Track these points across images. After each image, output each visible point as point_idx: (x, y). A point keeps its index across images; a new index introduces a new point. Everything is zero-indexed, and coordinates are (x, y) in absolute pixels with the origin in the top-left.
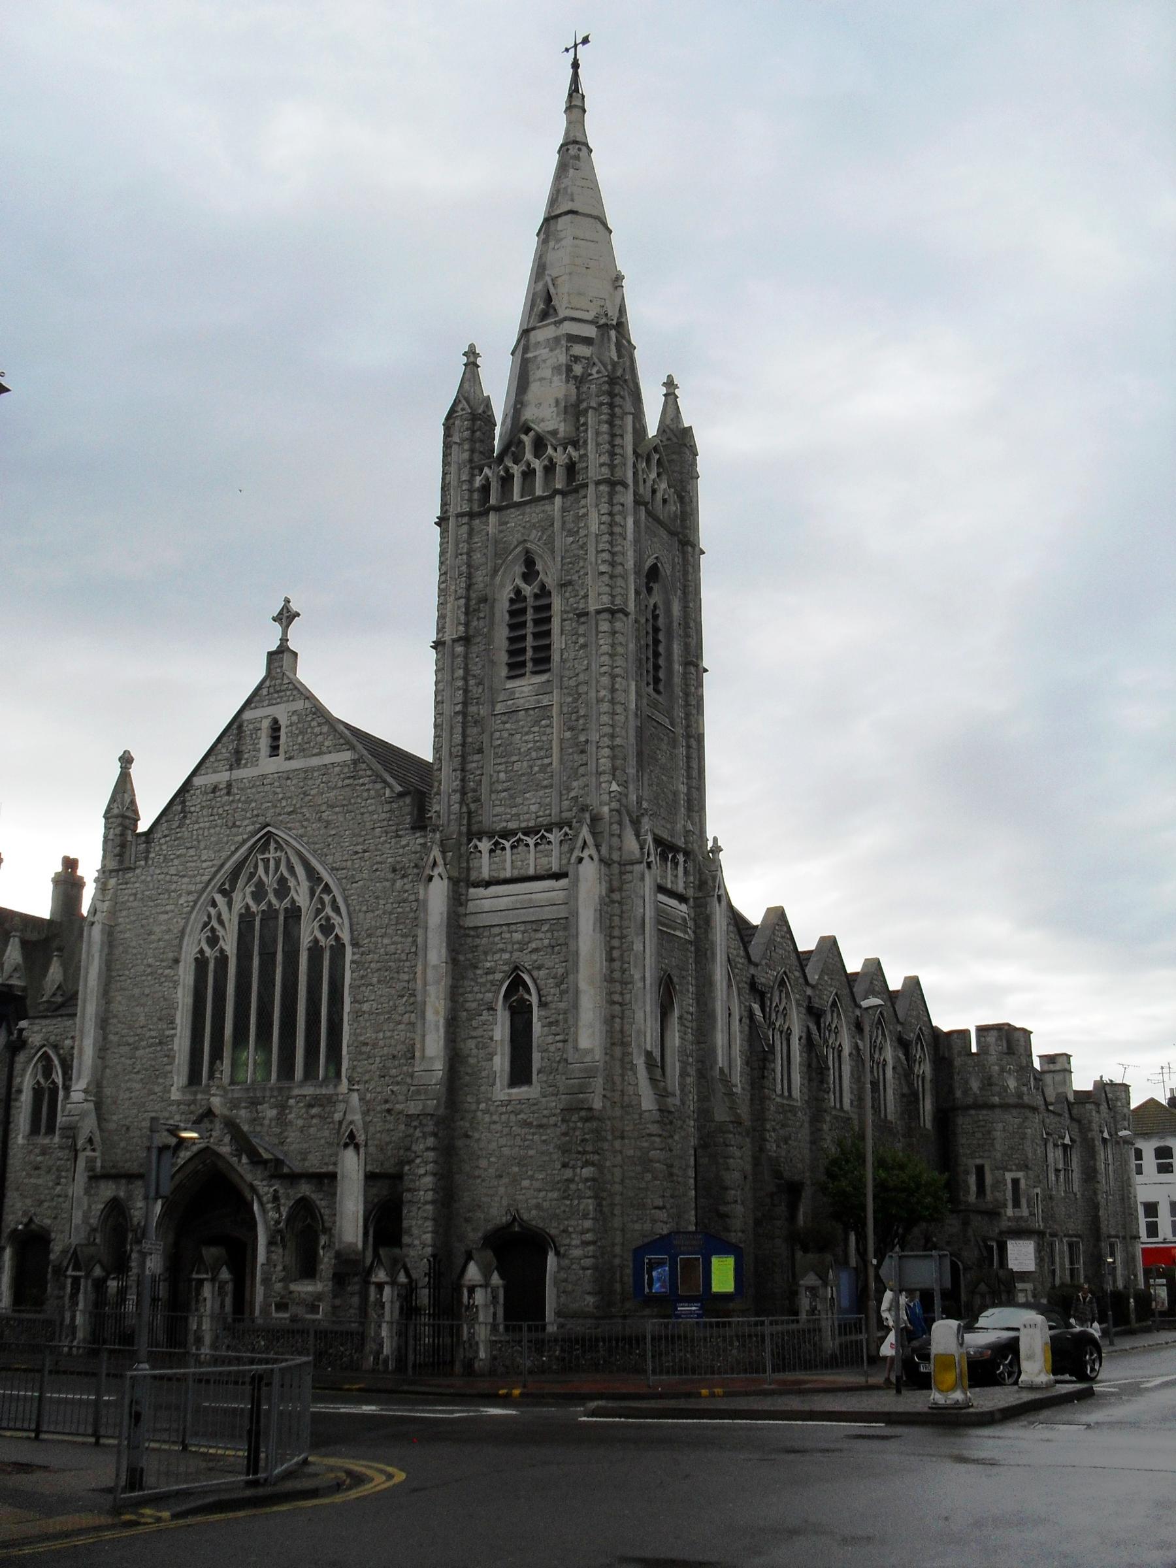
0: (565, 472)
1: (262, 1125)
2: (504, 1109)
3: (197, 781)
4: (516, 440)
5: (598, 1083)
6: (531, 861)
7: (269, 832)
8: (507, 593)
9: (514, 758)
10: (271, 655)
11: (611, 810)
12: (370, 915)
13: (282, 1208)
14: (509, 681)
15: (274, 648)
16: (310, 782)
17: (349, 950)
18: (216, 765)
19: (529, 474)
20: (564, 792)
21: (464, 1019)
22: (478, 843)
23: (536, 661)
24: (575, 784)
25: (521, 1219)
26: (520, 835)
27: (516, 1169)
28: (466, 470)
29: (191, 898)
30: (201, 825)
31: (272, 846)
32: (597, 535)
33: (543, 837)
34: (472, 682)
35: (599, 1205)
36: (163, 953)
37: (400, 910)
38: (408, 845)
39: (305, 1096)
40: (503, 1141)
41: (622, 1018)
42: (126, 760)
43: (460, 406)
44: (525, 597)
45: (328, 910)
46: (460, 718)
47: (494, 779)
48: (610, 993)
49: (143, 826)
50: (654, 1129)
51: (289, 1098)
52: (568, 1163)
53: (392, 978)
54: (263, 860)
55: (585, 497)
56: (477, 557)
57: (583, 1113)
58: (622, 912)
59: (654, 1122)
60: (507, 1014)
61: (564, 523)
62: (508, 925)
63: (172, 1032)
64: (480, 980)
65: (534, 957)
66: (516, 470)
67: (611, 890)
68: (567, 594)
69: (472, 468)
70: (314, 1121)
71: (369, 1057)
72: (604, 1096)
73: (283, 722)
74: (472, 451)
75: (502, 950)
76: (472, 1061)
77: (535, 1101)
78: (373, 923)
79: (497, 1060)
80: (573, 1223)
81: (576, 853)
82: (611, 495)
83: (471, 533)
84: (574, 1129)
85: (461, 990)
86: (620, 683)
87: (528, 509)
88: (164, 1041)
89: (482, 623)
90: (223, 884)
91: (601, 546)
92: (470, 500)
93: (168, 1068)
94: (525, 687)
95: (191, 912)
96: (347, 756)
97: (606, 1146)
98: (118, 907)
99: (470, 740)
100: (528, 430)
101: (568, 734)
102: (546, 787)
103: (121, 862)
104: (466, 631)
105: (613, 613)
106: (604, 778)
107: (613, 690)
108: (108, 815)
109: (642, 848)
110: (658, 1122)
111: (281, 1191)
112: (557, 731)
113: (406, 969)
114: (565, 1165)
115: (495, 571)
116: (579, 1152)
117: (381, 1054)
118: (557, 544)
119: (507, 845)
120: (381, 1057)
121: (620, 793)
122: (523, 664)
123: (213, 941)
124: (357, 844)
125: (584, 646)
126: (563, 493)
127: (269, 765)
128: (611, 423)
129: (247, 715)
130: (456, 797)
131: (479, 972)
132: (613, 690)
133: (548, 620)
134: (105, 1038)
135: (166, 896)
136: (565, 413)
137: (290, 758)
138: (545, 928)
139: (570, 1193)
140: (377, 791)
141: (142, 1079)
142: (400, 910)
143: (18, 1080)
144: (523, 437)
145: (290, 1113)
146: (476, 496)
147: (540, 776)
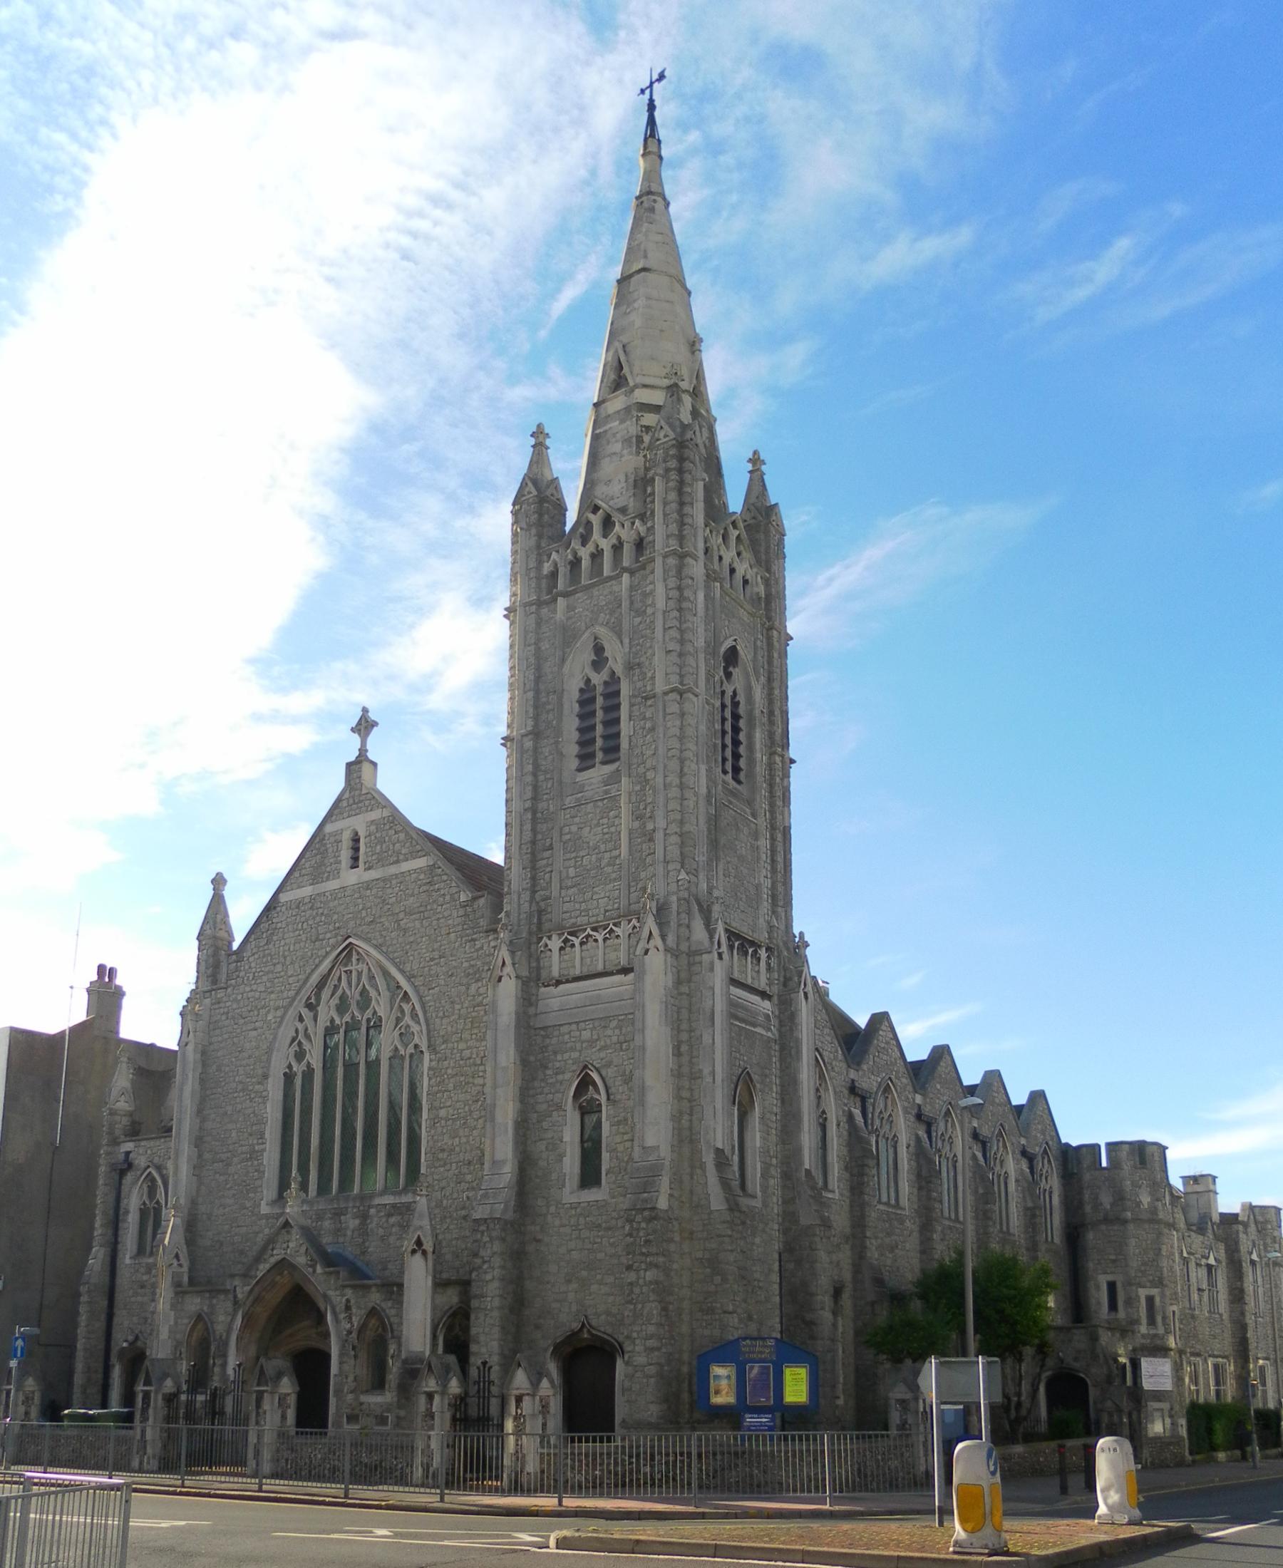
0: (634, 547)
2: (573, 1212)
3: (283, 898)
4: (584, 521)
5: (664, 1183)
6: (599, 955)
7: (350, 943)
9: (581, 854)
10: (349, 765)
11: (679, 900)
12: (445, 1021)
13: (354, 1318)
14: (579, 774)
15: (352, 759)
16: (389, 891)
17: (427, 1057)
18: (301, 879)
19: (597, 556)
20: (632, 884)
21: (534, 1121)
22: (548, 942)
23: (606, 751)
24: (643, 875)
25: (590, 1326)
27: (584, 1273)
28: (533, 557)
29: (279, 1013)
30: (287, 941)
31: (355, 957)
32: (664, 612)
33: (612, 931)
34: (541, 778)
35: (665, 1309)
36: (253, 1069)
37: (474, 1014)
38: (482, 948)
39: (386, 1205)
40: (572, 1245)
41: (691, 1115)
42: (219, 882)
43: (527, 489)
44: (595, 685)
45: (407, 1019)
46: (529, 816)
47: (564, 875)
48: (679, 1089)
49: (235, 946)
51: (370, 1207)
52: (632, 1266)
53: (468, 1083)
54: (346, 972)
55: (653, 572)
56: (545, 646)
57: (646, 1213)
58: (690, 1004)
59: (724, 1222)
61: (632, 603)
63: (263, 1146)
64: (550, 1081)
65: (602, 1055)
66: (585, 553)
67: (678, 982)
68: (636, 678)
69: (539, 554)
70: (394, 1230)
71: (445, 1164)
72: (671, 1195)
73: (362, 834)
74: (540, 536)
76: (542, 1163)
77: (603, 1203)
78: (449, 1028)
79: (567, 1160)
80: (637, 1328)
81: (642, 945)
82: (680, 569)
83: (539, 624)
84: (638, 1230)
85: (531, 1092)
86: (691, 766)
87: (595, 592)
88: (254, 1155)
89: (551, 716)
90: (309, 998)
91: (669, 624)
92: (539, 587)
93: (258, 1183)
96: (421, 863)
97: (672, 1247)
99: (539, 837)
100: (596, 509)
101: (636, 824)
102: (615, 880)
104: (536, 725)
107: (682, 774)
108: (200, 937)
109: (711, 937)
111: (353, 1302)
112: (625, 821)
113: (481, 1074)
114: (629, 1268)
115: (563, 660)
116: (643, 1254)
117: (457, 1160)
118: (626, 626)
119: (577, 941)
120: (457, 1163)
122: (592, 756)
123: (300, 1055)
124: (433, 950)
125: (653, 729)
126: (632, 572)
127: (351, 877)
128: (680, 492)
129: (329, 828)
130: (526, 896)
131: (549, 1072)
132: (682, 774)
133: (617, 707)
134: (200, 1156)
135: (256, 1013)
136: (635, 486)
137: (369, 868)
138: (614, 1024)
139: (634, 1297)
141: (234, 1195)
142: (474, 1014)
143: (125, 1201)
144: (591, 517)
145: (371, 1223)
146: (544, 583)
147: (609, 869)
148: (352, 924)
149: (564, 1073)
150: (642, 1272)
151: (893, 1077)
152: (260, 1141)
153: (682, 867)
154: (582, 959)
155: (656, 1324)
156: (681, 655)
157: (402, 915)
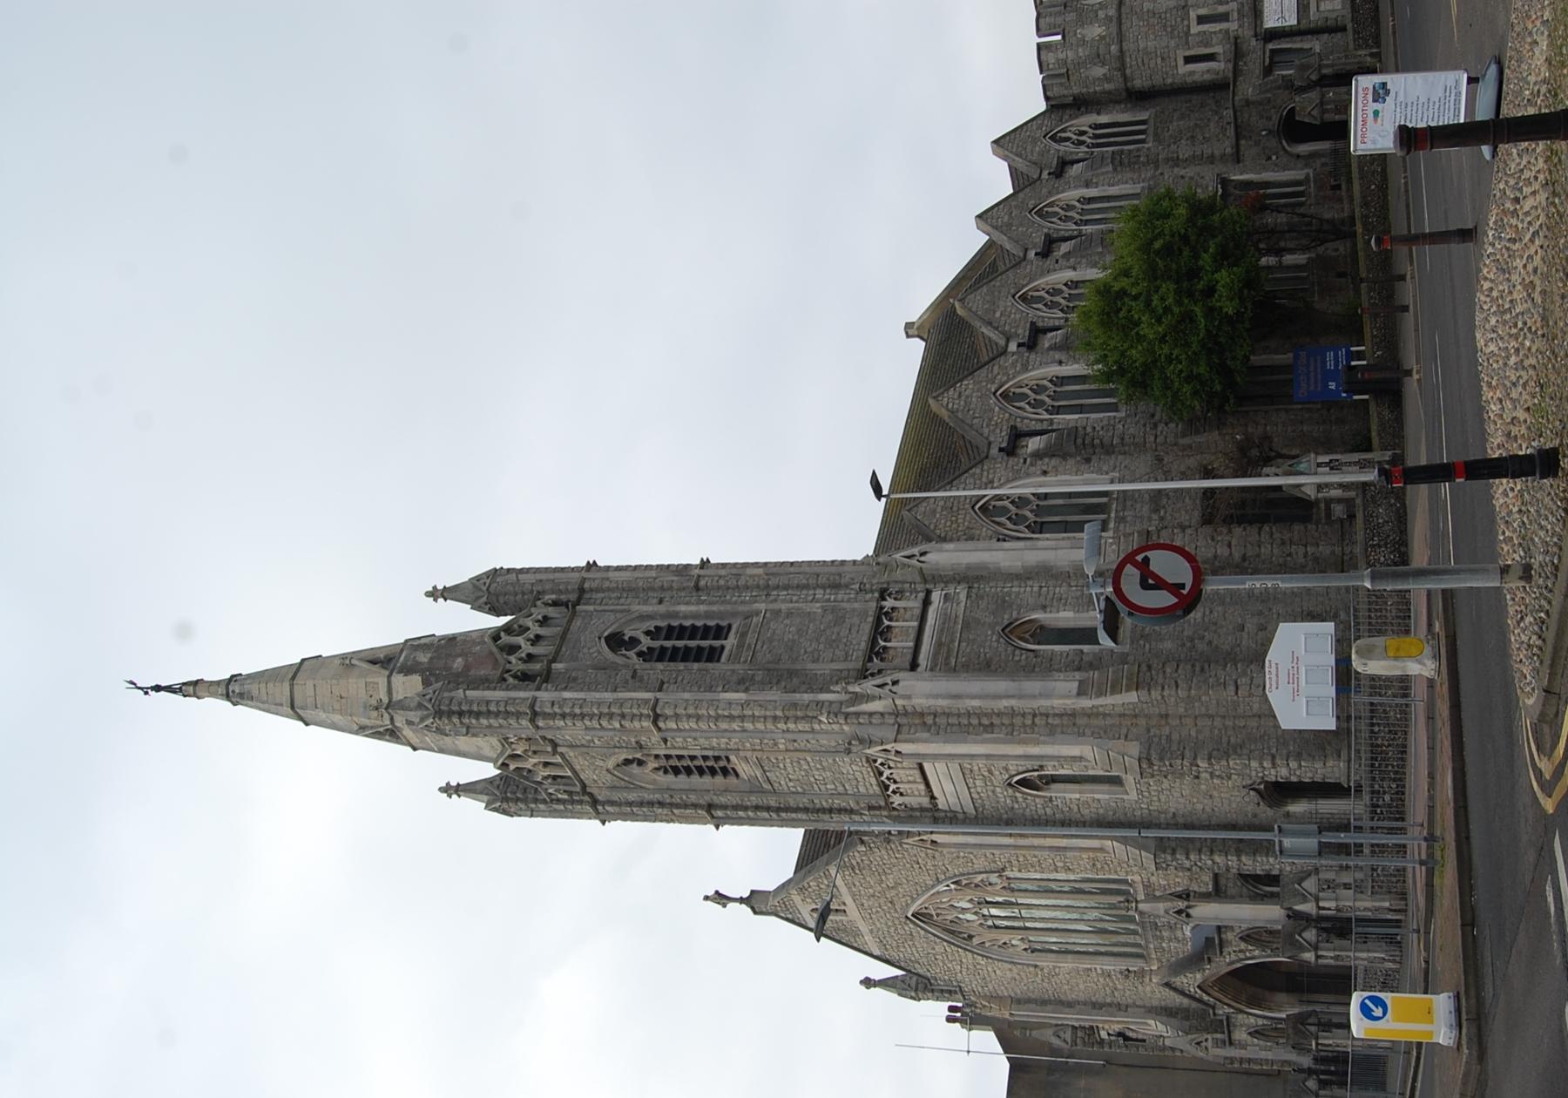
7: (913, 915)
8: (661, 778)
9: (812, 779)
16: (862, 892)
26: (883, 778)
41: (1047, 715)
46: (783, 815)
50: (1155, 694)
60: (1054, 786)
62: (969, 788)
69: (552, 800)
74: (536, 801)
75: (993, 792)
82: (546, 716)
90: (964, 938)
94: (744, 769)
95: (991, 958)
97: (1175, 737)
98: (995, 995)
103: (956, 992)
105: (656, 719)
106: (817, 727)
107: (731, 718)
110: (1149, 690)
121: (829, 713)
131: (1016, 806)
140: (862, 856)
144: (512, 767)
148: (897, 915)
149: (1016, 797)
150: (1201, 769)
151: (993, 390)
153: (816, 718)
154: (909, 782)
155: (1249, 760)
156: (623, 716)
157: (884, 885)
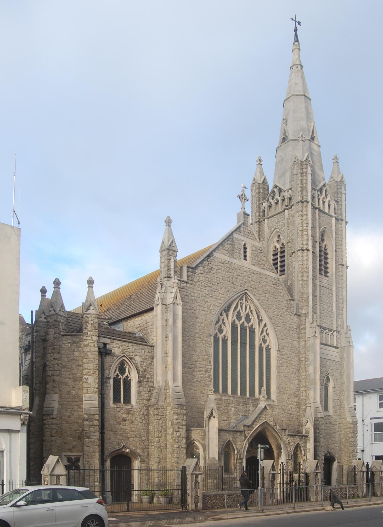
1: (249, 413)
152: (209, 364)
